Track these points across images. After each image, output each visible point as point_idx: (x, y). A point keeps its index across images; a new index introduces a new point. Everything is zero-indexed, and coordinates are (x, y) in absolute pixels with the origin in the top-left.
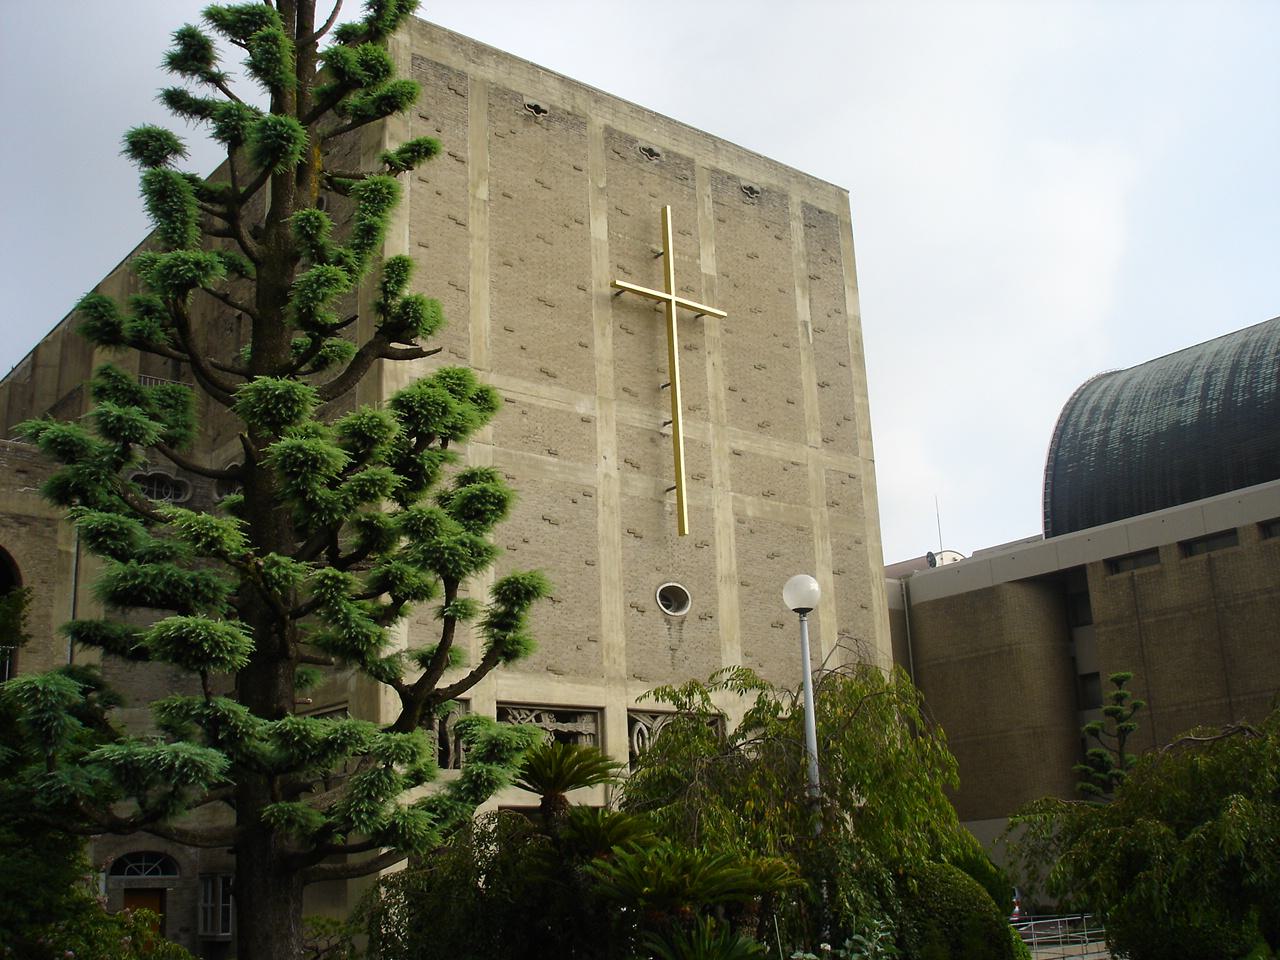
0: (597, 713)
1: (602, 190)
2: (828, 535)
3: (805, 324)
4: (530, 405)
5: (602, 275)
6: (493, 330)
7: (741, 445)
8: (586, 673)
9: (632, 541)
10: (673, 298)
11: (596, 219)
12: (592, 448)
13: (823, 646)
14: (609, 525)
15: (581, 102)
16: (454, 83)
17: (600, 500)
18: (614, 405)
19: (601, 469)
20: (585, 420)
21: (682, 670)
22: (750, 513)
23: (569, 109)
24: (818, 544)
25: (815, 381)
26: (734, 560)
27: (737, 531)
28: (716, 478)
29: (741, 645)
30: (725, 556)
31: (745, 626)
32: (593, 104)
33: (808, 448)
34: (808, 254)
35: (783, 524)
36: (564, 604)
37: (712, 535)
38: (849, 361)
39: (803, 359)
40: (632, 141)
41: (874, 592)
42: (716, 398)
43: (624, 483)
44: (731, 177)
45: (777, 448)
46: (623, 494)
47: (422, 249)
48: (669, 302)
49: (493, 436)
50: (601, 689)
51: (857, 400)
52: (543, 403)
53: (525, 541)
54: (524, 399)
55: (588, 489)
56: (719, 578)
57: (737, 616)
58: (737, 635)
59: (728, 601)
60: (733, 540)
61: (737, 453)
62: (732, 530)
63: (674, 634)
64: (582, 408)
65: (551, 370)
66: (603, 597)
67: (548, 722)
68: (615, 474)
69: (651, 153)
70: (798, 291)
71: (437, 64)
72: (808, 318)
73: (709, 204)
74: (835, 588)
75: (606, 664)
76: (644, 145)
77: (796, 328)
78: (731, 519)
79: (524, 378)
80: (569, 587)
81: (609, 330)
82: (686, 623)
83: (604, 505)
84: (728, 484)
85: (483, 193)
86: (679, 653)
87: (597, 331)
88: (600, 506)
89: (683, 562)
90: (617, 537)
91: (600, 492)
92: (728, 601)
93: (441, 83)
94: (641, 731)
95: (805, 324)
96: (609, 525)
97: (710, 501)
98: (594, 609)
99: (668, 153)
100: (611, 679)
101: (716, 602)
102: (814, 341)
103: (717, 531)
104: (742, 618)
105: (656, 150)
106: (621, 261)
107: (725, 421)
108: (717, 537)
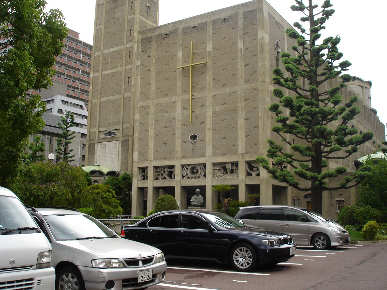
0: (173, 167)
1: (181, 45)
2: (244, 109)
3: (241, 50)
4: (162, 103)
5: (180, 65)
6: (155, 90)
7: (216, 93)
8: (171, 158)
9: (184, 127)
10: (191, 65)
11: (179, 53)
12: (175, 108)
13: (239, 141)
14: (178, 125)
15: (177, 26)
16: (149, 40)
17: (177, 120)
18: (181, 96)
19: (177, 112)
20: (174, 102)
21: (195, 154)
22: (217, 110)
23: (174, 29)
24: (239, 113)
25: (243, 64)
26: (211, 124)
27: (213, 117)
28: (208, 104)
29: (212, 145)
30: (209, 124)
31: (214, 140)
32: (180, 24)
33: (239, 86)
34: (244, 27)
35: (228, 110)
36: (167, 144)
37: (206, 120)
38: (258, 53)
39: (239, 60)
40: (189, 27)
41: (260, 121)
42: (209, 83)
43: (183, 113)
44: (218, 20)
45: (228, 90)
46: (182, 116)
47: (143, 80)
48: (192, 66)
49: (154, 113)
50: (175, 161)
51: (260, 64)
52: (165, 102)
53: (160, 133)
54: (161, 102)
55: (174, 118)
56: (206, 130)
57: (211, 139)
58: (211, 143)
59: (209, 136)
60: (211, 119)
61: (214, 96)
62: (211, 116)
63: (193, 146)
64: (173, 100)
65: (167, 94)
66: (176, 141)
67: (166, 169)
68: (180, 112)
69: (194, 27)
70: (239, 41)
71: (146, 38)
72: (242, 47)
73: (211, 31)
74: (245, 124)
75: (176, 156)
76: (193, 26)
77: (238, 52)
78: (211, 113)
79: (161, 98)
80: (169, 140)
81: (181, 78)
82: (197, 143)
83: (177, 120)
84: (211, 105)
85: (154, 61)
86: (194, 150)
87: (178, 80)
88: (177, 121)
89: (197, 128)
90: (180, 126)
91: (177, 117)
92: (209, 136)
93: (147, 42)
94: (184, 169)
95: (241, 50)
96: (178, 125)
97: (205, 111)
98: (174, 144)
99: (199, 24)
100: (177, 159)
101: (205, 136)
102: (244, 53)
103: (207, 118)
104: (213, 138)
105: (196, 25)
106: (185, 60)
107: (211, 88)
108: (207, 120)
